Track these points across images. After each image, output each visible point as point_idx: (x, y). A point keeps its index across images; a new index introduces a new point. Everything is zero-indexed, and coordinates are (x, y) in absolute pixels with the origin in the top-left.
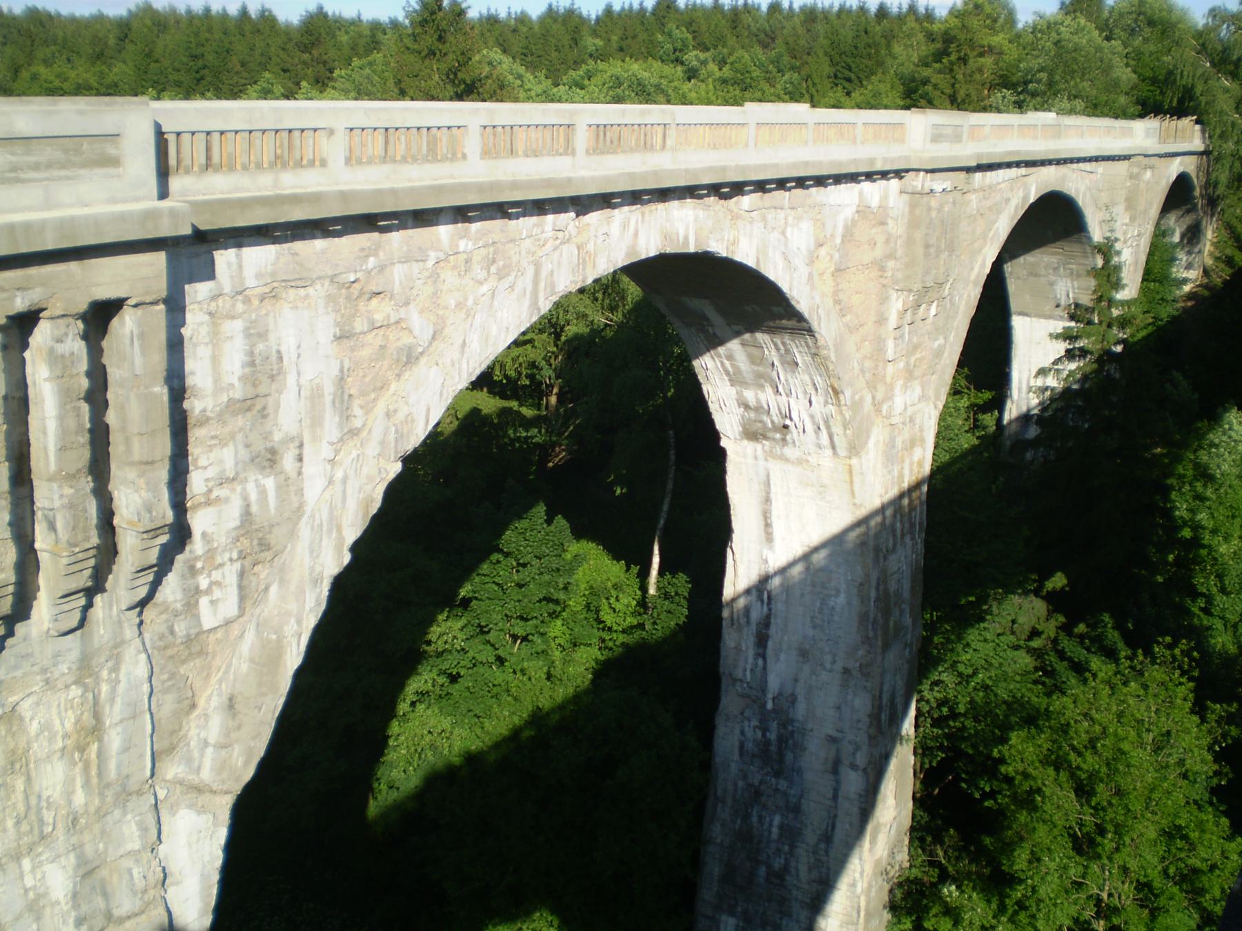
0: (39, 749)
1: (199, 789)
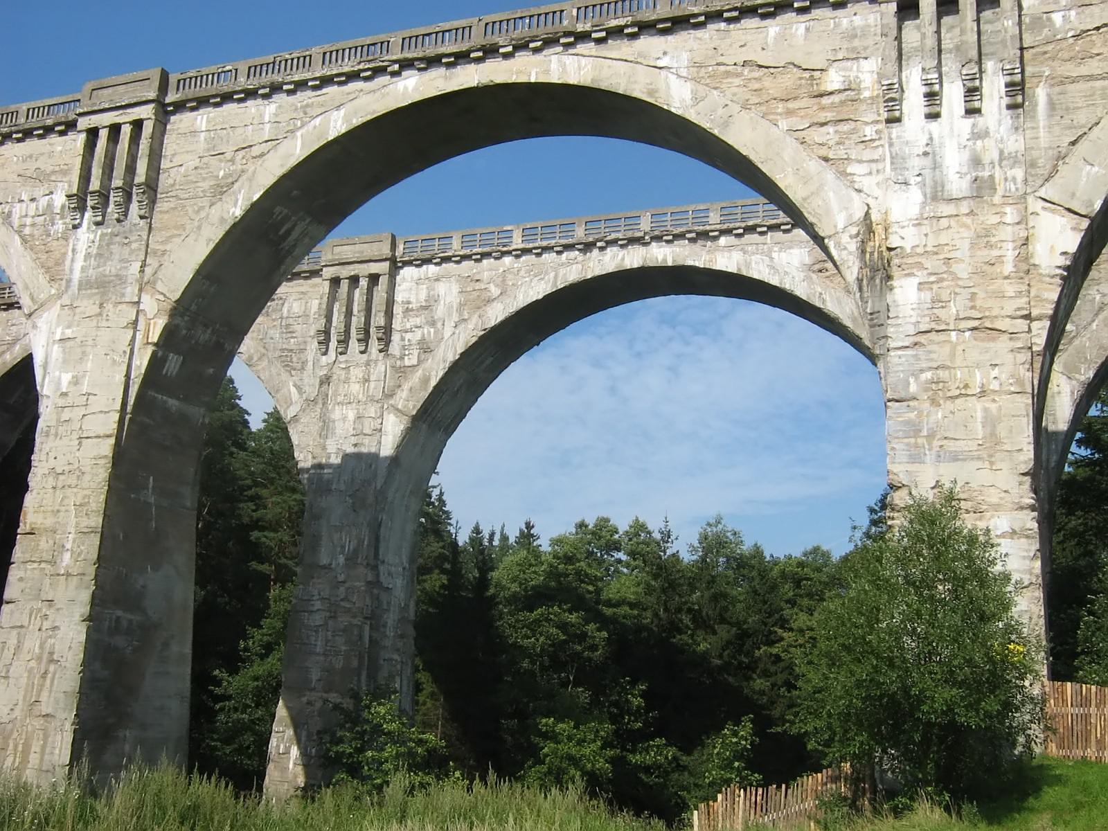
0: (353, 379)
1: (397, 409)
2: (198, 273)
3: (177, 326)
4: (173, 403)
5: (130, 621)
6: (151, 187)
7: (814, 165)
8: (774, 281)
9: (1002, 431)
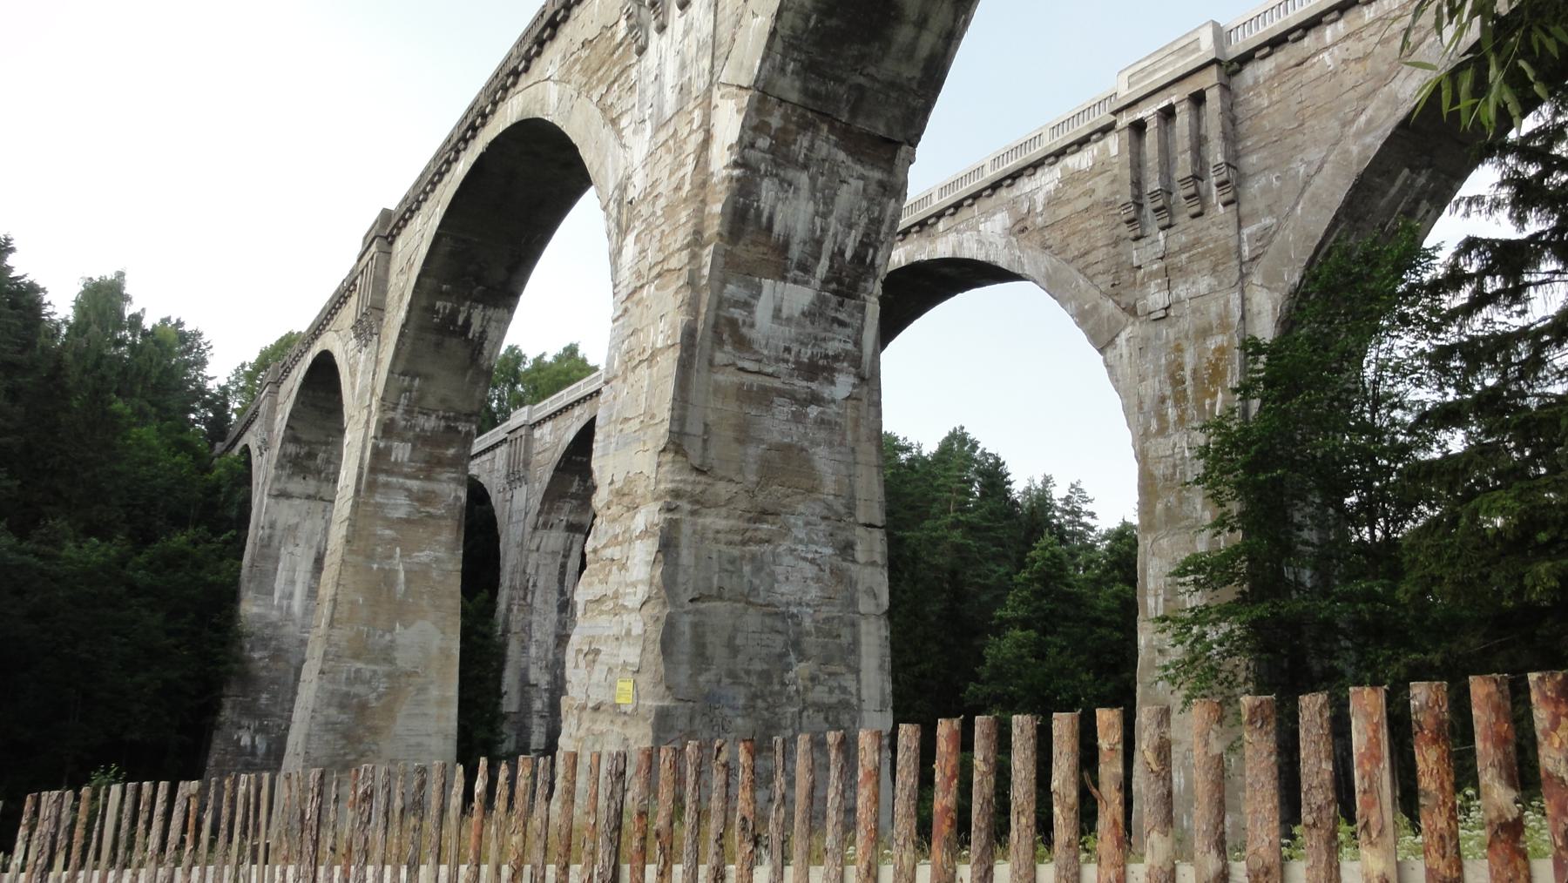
2: (391, 372)
3: (392, 420)
4: (414, 484)
5: (375, 672)
8: (981, 257)
9: (655, 403)
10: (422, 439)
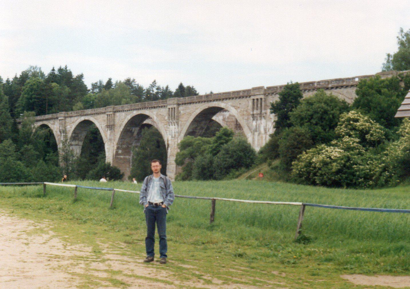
4: (122, 157)
6: (114, 125)
7: (164, 131)
10: (123, 149)
